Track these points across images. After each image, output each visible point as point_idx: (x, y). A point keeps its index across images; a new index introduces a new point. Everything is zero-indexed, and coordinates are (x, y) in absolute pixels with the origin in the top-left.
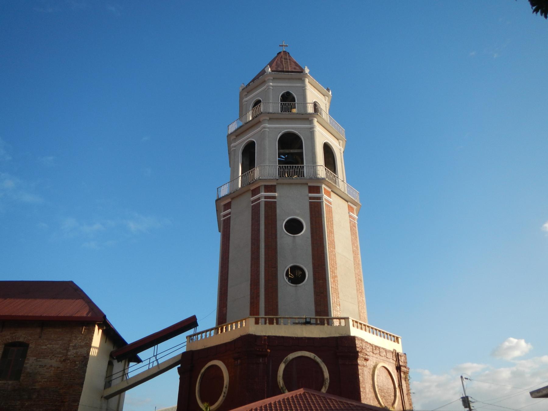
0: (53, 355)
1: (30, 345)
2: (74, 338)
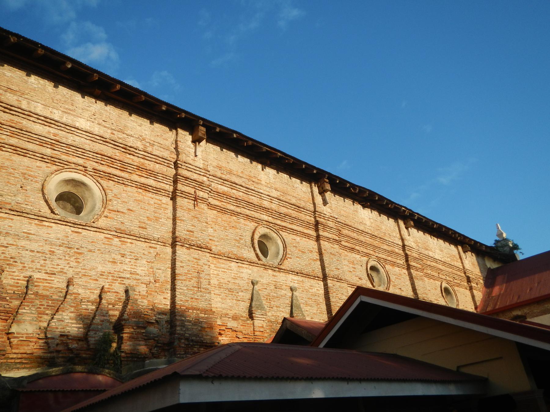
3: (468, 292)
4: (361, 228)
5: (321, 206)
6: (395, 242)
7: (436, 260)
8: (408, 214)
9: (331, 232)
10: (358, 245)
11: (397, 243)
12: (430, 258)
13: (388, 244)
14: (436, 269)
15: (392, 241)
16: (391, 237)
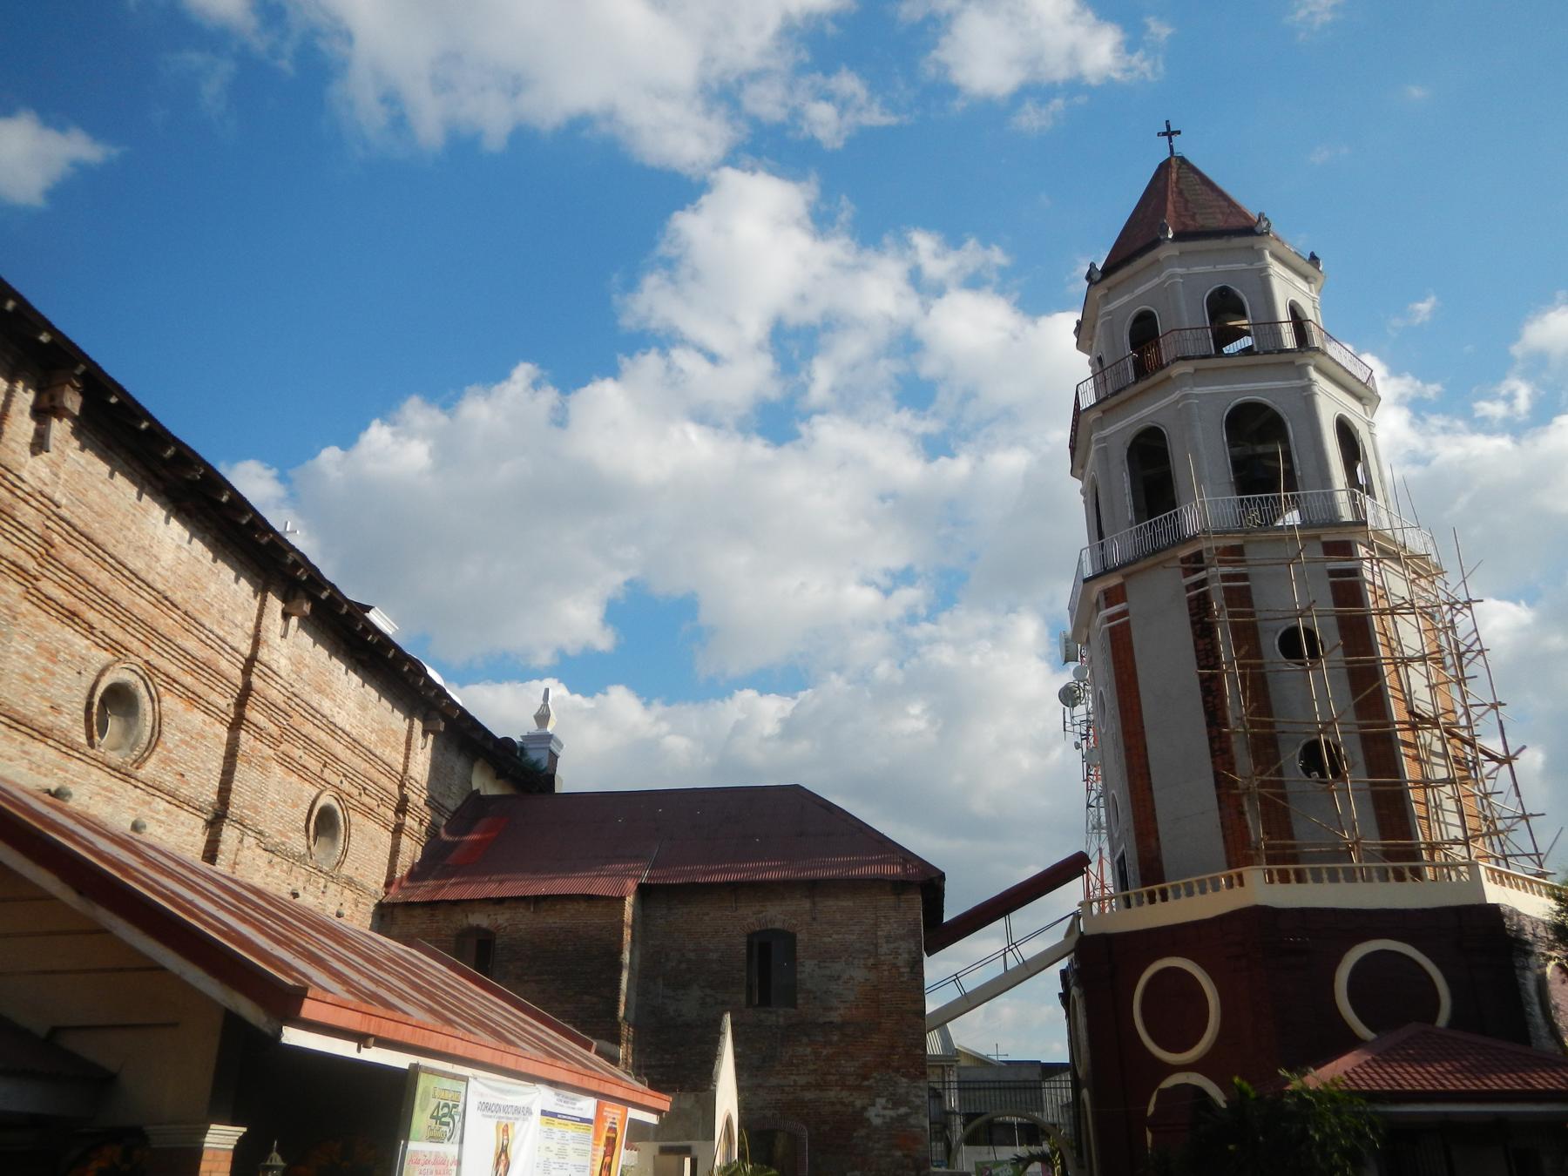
0: (849, 956)
1: (798, 935)
2: (883, 920)
3: (386, 838)
4: (137, 563)
5: (18, 449)
6: (229, 639)
7: (333, 729)
8: (304, 578)
9: (15, 540)
10: (98, 607)
11: (235, 645)
12: (318, 716)
13: (203, 638)
14: (322, 751)
15: (221, 634)
16: (225, 622)
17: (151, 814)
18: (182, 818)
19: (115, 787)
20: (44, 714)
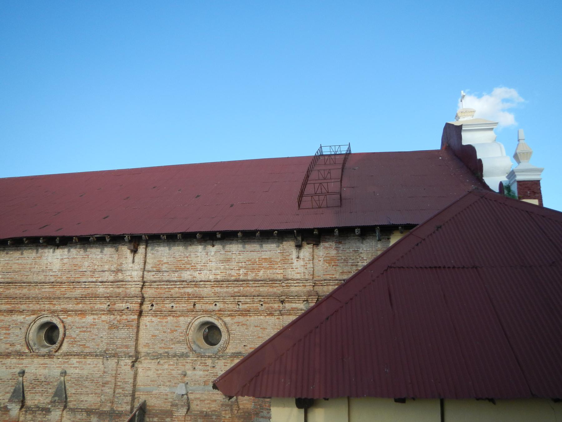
4: (41, 278)
6: (100, 279)
7: (195, 283)
10: (24, 303)
12: (178, 283)
13: (83, 286)
15: (94, 280)
17: (69, 366)
18: (89, 362)
19: (48, 362)
20: (8, 349)
